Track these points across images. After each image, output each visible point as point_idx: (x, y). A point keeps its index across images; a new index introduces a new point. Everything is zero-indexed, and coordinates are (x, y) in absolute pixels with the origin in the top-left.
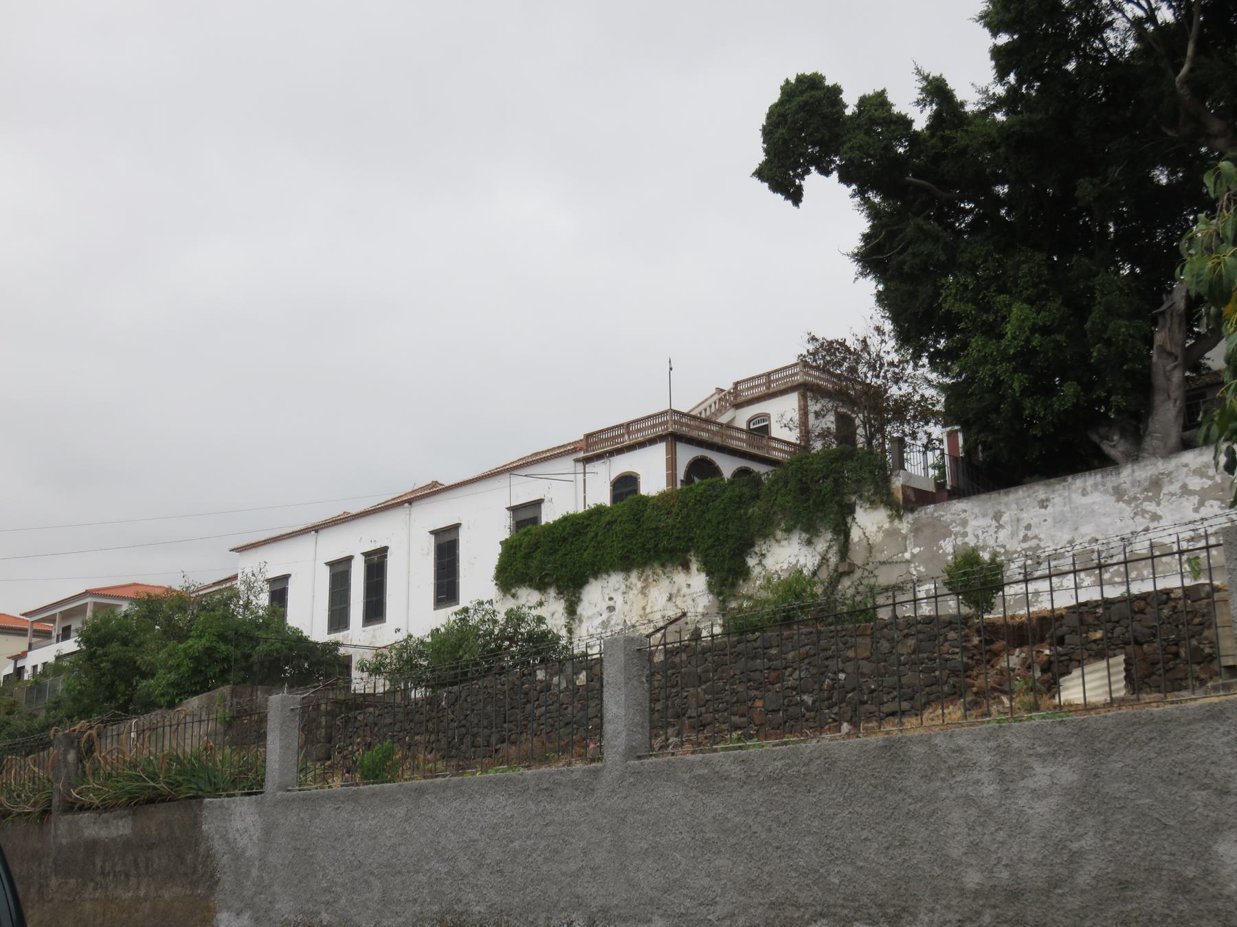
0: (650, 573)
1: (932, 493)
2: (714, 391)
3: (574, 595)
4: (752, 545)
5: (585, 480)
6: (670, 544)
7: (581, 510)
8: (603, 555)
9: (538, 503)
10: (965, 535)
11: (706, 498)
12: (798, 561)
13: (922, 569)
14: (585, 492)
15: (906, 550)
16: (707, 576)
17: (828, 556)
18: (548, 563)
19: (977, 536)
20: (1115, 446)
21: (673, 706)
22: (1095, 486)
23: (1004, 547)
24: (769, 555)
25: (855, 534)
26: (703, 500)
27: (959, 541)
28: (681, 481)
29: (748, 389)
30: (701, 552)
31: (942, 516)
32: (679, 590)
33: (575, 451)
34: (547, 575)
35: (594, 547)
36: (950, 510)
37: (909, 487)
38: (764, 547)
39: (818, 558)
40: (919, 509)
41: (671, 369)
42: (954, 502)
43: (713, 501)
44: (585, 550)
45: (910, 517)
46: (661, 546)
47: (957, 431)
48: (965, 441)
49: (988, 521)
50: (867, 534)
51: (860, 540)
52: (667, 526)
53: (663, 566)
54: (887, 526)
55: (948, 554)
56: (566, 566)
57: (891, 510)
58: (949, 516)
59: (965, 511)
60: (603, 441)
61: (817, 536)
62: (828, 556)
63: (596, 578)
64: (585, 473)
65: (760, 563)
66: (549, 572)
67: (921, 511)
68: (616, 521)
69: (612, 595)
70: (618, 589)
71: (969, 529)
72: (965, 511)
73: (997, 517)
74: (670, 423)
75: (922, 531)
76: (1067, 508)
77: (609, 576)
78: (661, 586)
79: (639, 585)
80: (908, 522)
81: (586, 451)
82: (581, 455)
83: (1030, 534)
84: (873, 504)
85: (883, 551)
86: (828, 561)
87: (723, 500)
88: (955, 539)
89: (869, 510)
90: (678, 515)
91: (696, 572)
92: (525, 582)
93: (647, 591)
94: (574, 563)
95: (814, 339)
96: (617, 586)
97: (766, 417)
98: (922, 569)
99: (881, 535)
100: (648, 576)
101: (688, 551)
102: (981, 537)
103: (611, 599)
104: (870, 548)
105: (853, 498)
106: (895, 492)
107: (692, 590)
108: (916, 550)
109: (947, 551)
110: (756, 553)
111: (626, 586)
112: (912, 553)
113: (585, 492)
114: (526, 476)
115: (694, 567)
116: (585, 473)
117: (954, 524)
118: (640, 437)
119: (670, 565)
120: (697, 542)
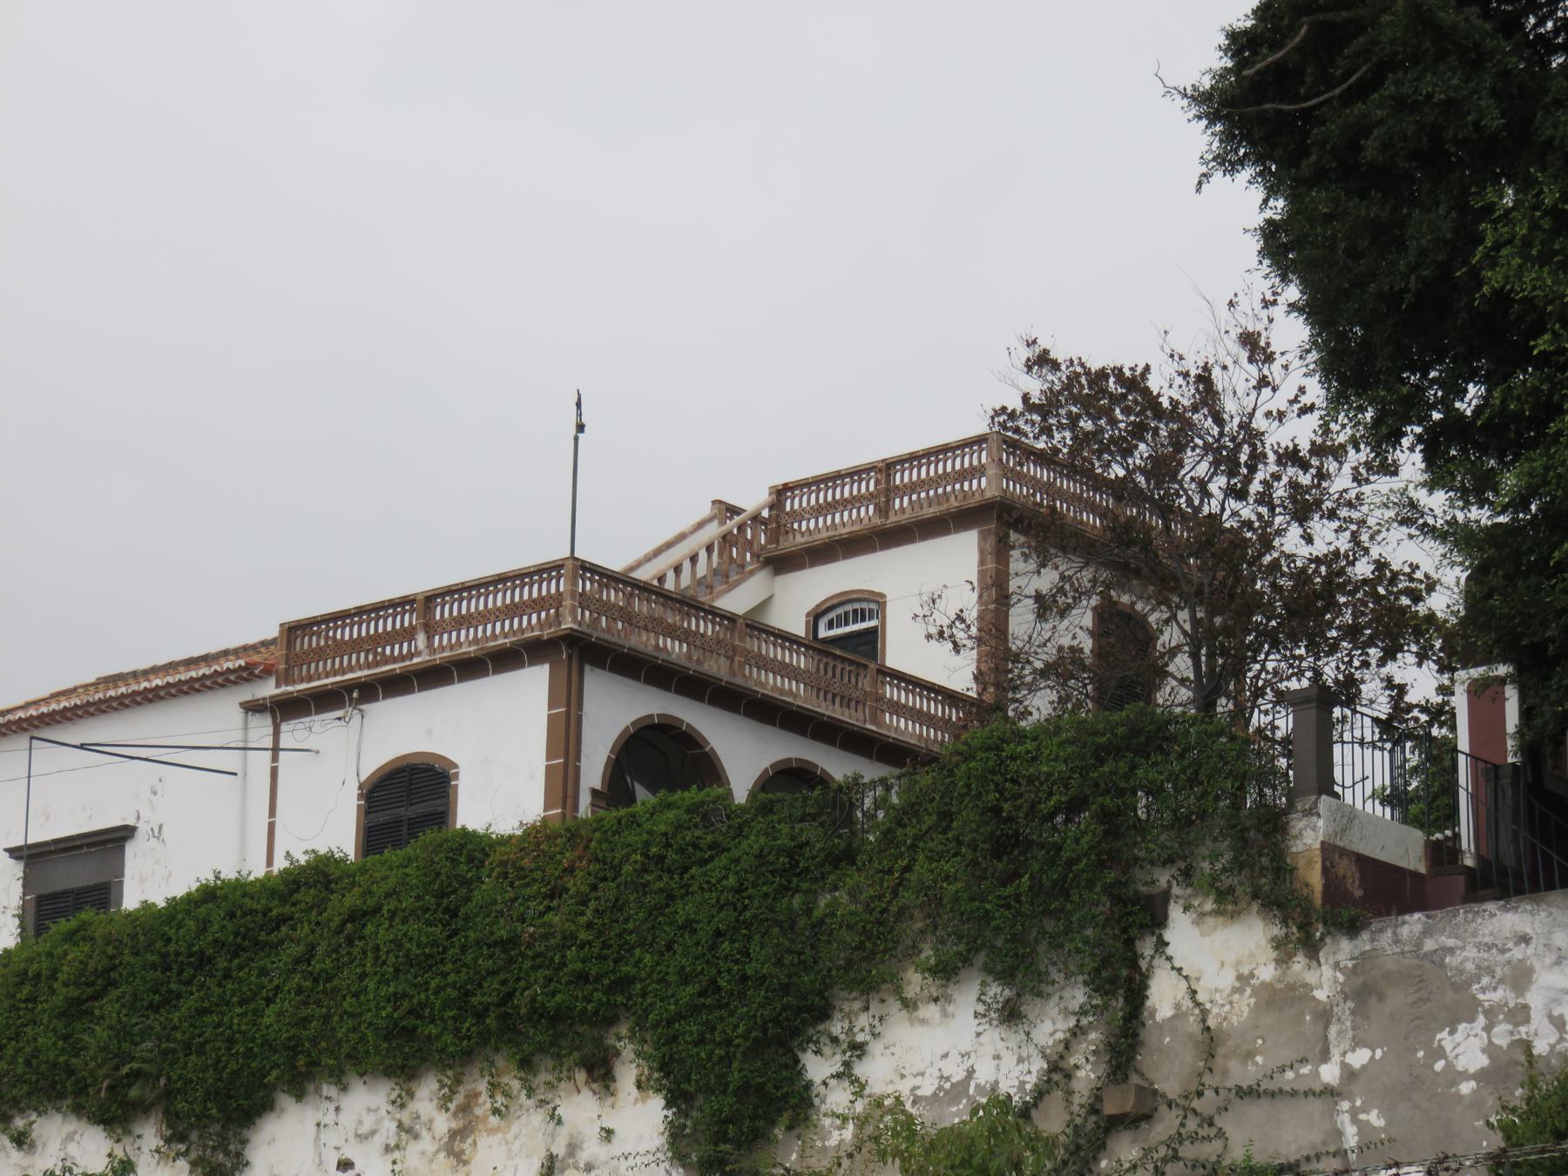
0: (482, 1086)
1: (1415, 875)
2: (706, 511)
3: (222, 1146)
4: (825, 1014)
5: (274, 773)
6: (553, 994)
7: (258, 871)
8: (327, 1018)
9: (114, 840)
10: (1520, 1014)
11: (681, 851)
12: (971, 1073)
13: (1375, 1118)
14: (272, 812)
15: (1325, 1056)
16: (668, 1106)
17: (1072, 1061)
18: (144, 1035)
24: (875, 1048)
25: (1163, 995)
26: (671, 855)
27: (1502, 1035)
28: (594, 792)
29: (819, 510)
30: (655, 1026)
31: (1451, 951)
32: (573, 1148)
33: (246, 675)
34: (136, 1075)
35: (299, 991)
36: (1475, 935)
37: (1344, 852)
38: (863, 1020)
39: (1038, 1065)
40: (1375, 926)
41: (580, 428)
42: (1491, 906)
43: (703, 862)
44: (269, 1001)
45: (1344, 949)
46: (522, 1000)
47: (1502, 681)
48: (1526, 714)
50: (1201, 997)
51: (1179, 1015)
52: (545, 937)
53: (526, 1065)
54: (1267, 973)
55: (1464, 1076)
56: (201, 1051)
57: (1285, 922)
58: (1471, 953)
59: (1525, 939)
60: (341, 648)
61: (1039, 994)
62: (1072, 1061)
63: (300, 1096)
64: (276, 750)
65: (846, 1074)
66: (146, 1067)
67: (1381, 931)
68: (377, 910)
69: (349, 1153)
70: (373, 1133)
71: (1535, 999)
72: (1525, 939)
74: (567, 602)
75: (1382, 998)
77: (344, 1089)
78: (515, 1128)
79: (443, 1123)
80: (1336, 966)
81: (285, 678)
82: (268, 689)
84: (1227, 903)
85: (1250, 1055)
87: (737, 861)
88: (1488, 1029)
89: (1210, 921)
90: (584, 903)
91: (634, 1091)
92: (61, 1096)
93: (466, 1146)
94: (231, 1041)
95: (1043, 361)
97: (871, 604)
98: (1375, 1118)
99: (1245, 1002)
100: (473, 1096)
101: (612, 1021)
104: (1210, 1042)
105: (1163, 878)
106: (1301, 864)
107: (617, 1147)
108: (1359, 1058)
109: (1461, 1065)
110: (835, 1040)
111: (400, 1125)
112: (1345, 1066)
113: (272, 812)
114: (82, 747)
115: (627, 1074)
116: (276, 750)
117: (1486, 980)
118: (465, 642)
119: (550, 1063)
120: (644, 994)
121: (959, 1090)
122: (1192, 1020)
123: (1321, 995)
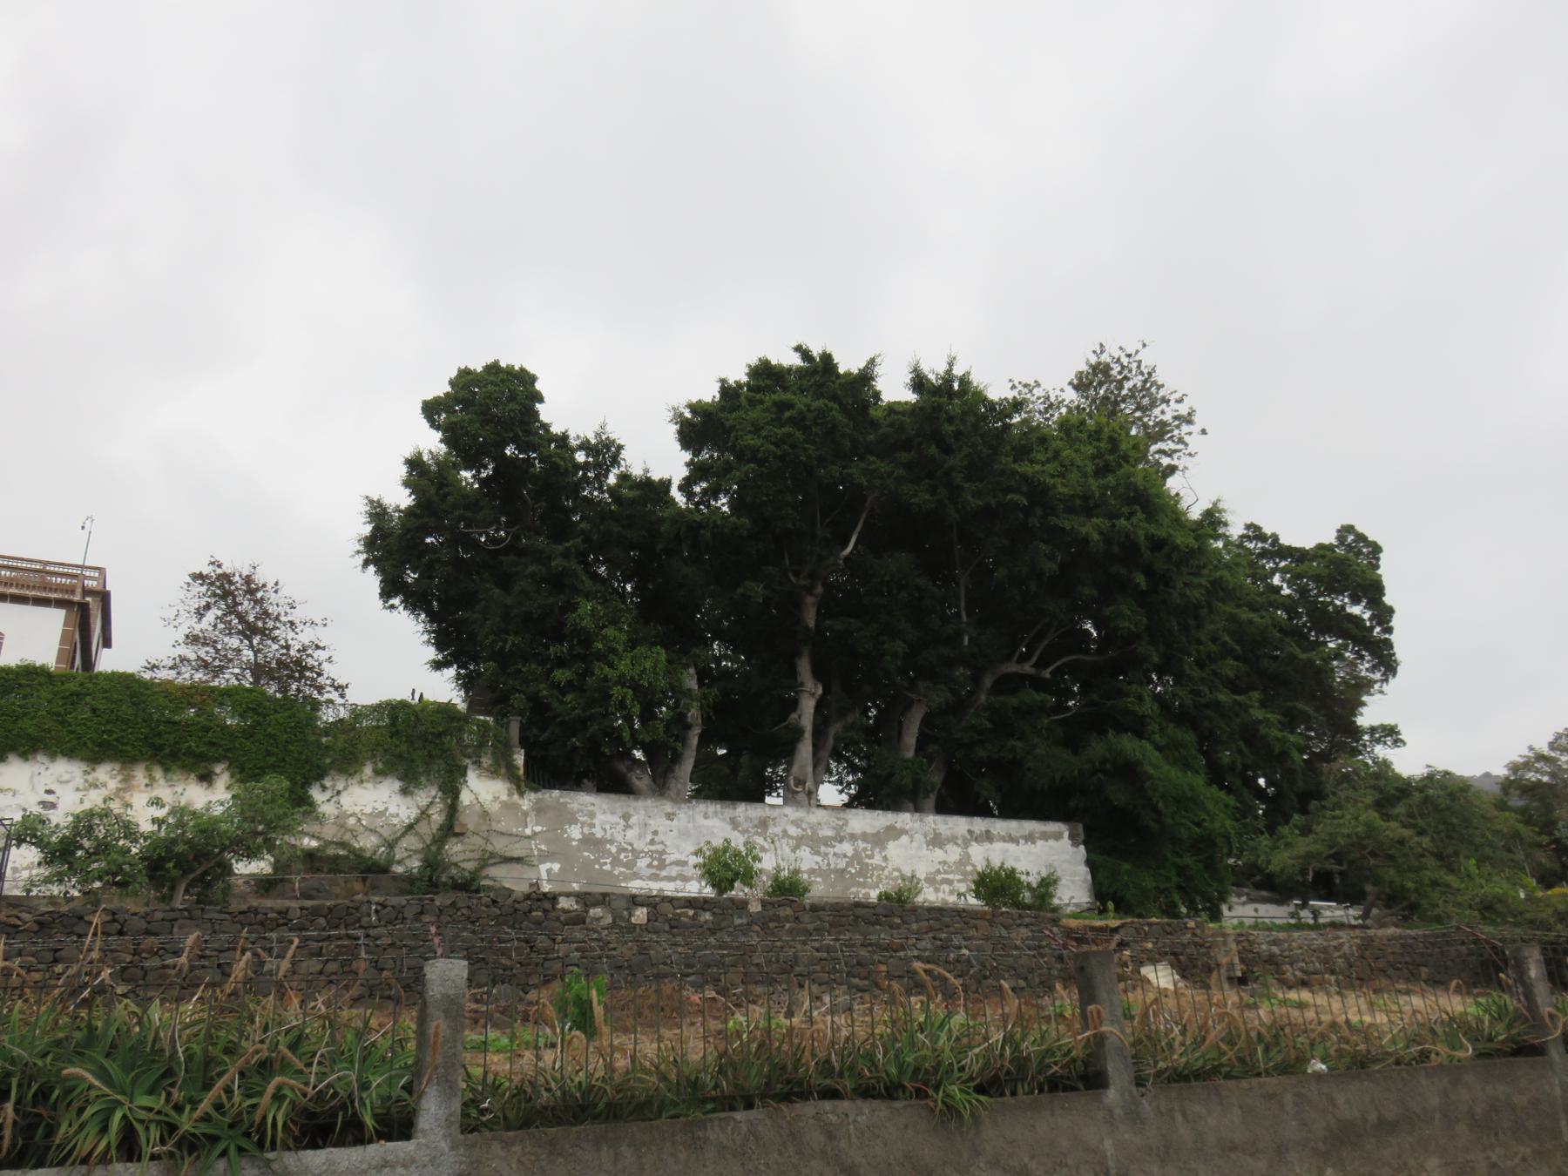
10: (592, 826)
12: (387, 809)
13: (543, 847)
15: (526, 826)
19: (605, 830)
20: (641, 780)
21: (778, 961)
22: (716, 813)
23: (631, 845)
24: (344, 794)
25: (465, 798)
27: (586, 831)
45: (533, 796)
49: (615, 819)
51: (471, 805)
53: (167, 770)
54: (504, 798)
71: (596, 821)
73: (626, 817)
76: (690, 825)
83: (656, 839)
84: (493, 773)
85: (499, 822)
86: (429, 816)
96: (66, 777)
101: (217, 760)
102: (609, 832)
103: (49, 792)
104: (485, 814)
108: (538, 829)
121: (382, 814)
122: (477, 807)
123: (525, 808)
